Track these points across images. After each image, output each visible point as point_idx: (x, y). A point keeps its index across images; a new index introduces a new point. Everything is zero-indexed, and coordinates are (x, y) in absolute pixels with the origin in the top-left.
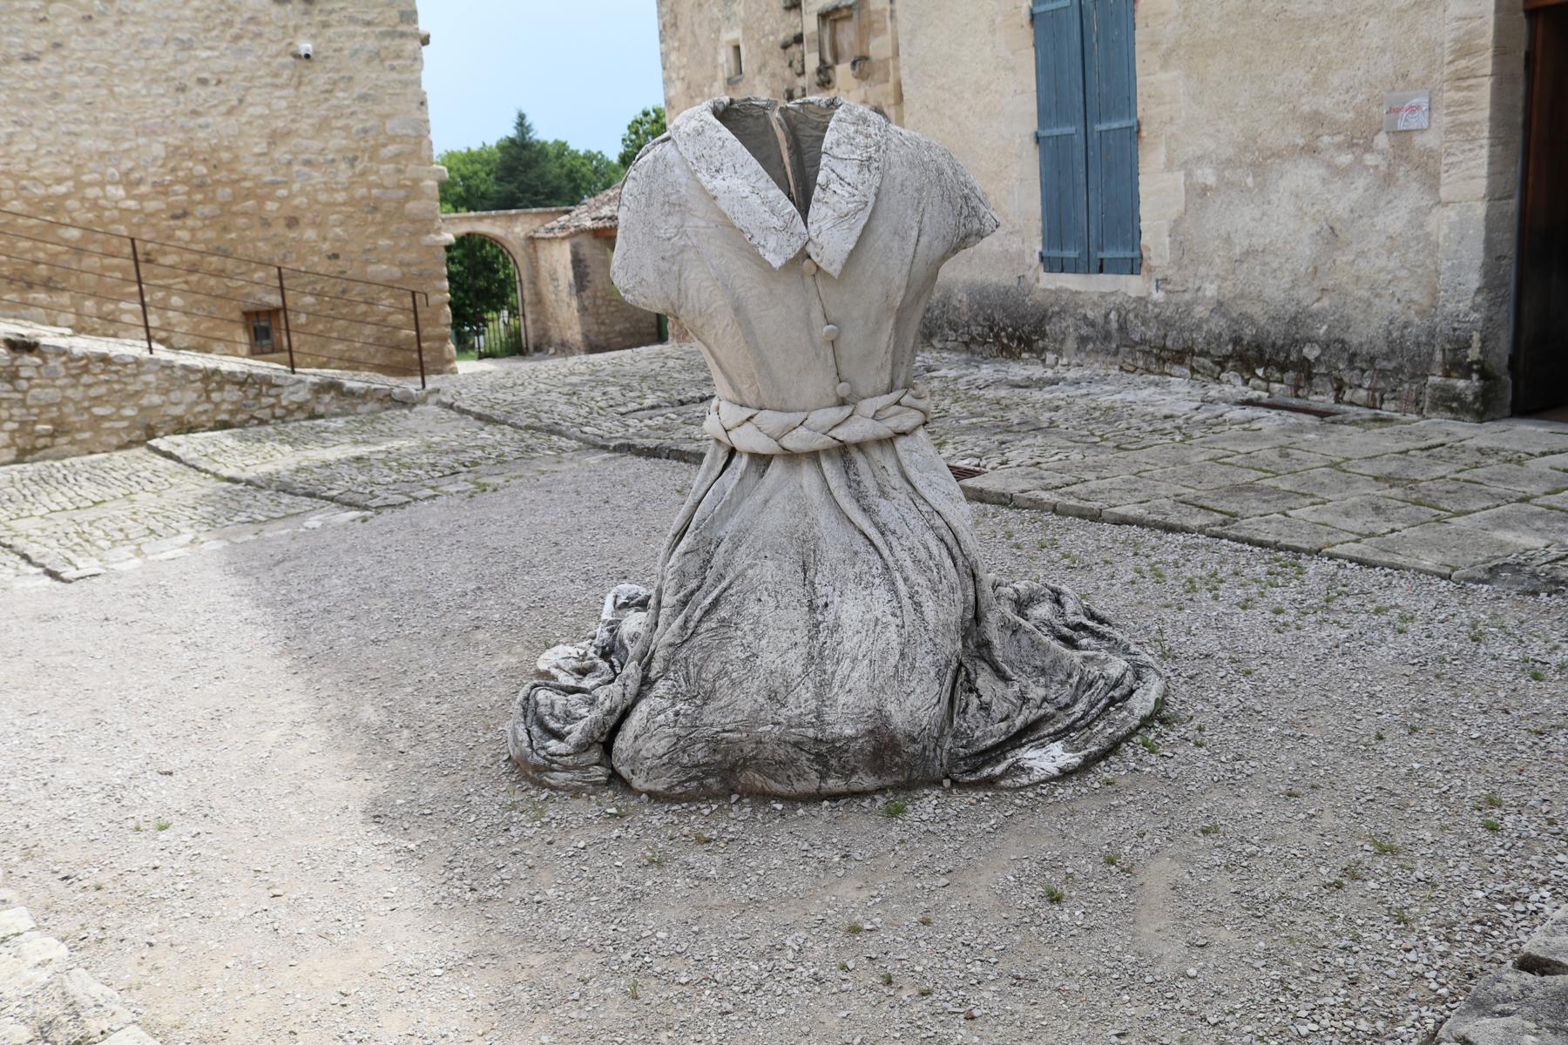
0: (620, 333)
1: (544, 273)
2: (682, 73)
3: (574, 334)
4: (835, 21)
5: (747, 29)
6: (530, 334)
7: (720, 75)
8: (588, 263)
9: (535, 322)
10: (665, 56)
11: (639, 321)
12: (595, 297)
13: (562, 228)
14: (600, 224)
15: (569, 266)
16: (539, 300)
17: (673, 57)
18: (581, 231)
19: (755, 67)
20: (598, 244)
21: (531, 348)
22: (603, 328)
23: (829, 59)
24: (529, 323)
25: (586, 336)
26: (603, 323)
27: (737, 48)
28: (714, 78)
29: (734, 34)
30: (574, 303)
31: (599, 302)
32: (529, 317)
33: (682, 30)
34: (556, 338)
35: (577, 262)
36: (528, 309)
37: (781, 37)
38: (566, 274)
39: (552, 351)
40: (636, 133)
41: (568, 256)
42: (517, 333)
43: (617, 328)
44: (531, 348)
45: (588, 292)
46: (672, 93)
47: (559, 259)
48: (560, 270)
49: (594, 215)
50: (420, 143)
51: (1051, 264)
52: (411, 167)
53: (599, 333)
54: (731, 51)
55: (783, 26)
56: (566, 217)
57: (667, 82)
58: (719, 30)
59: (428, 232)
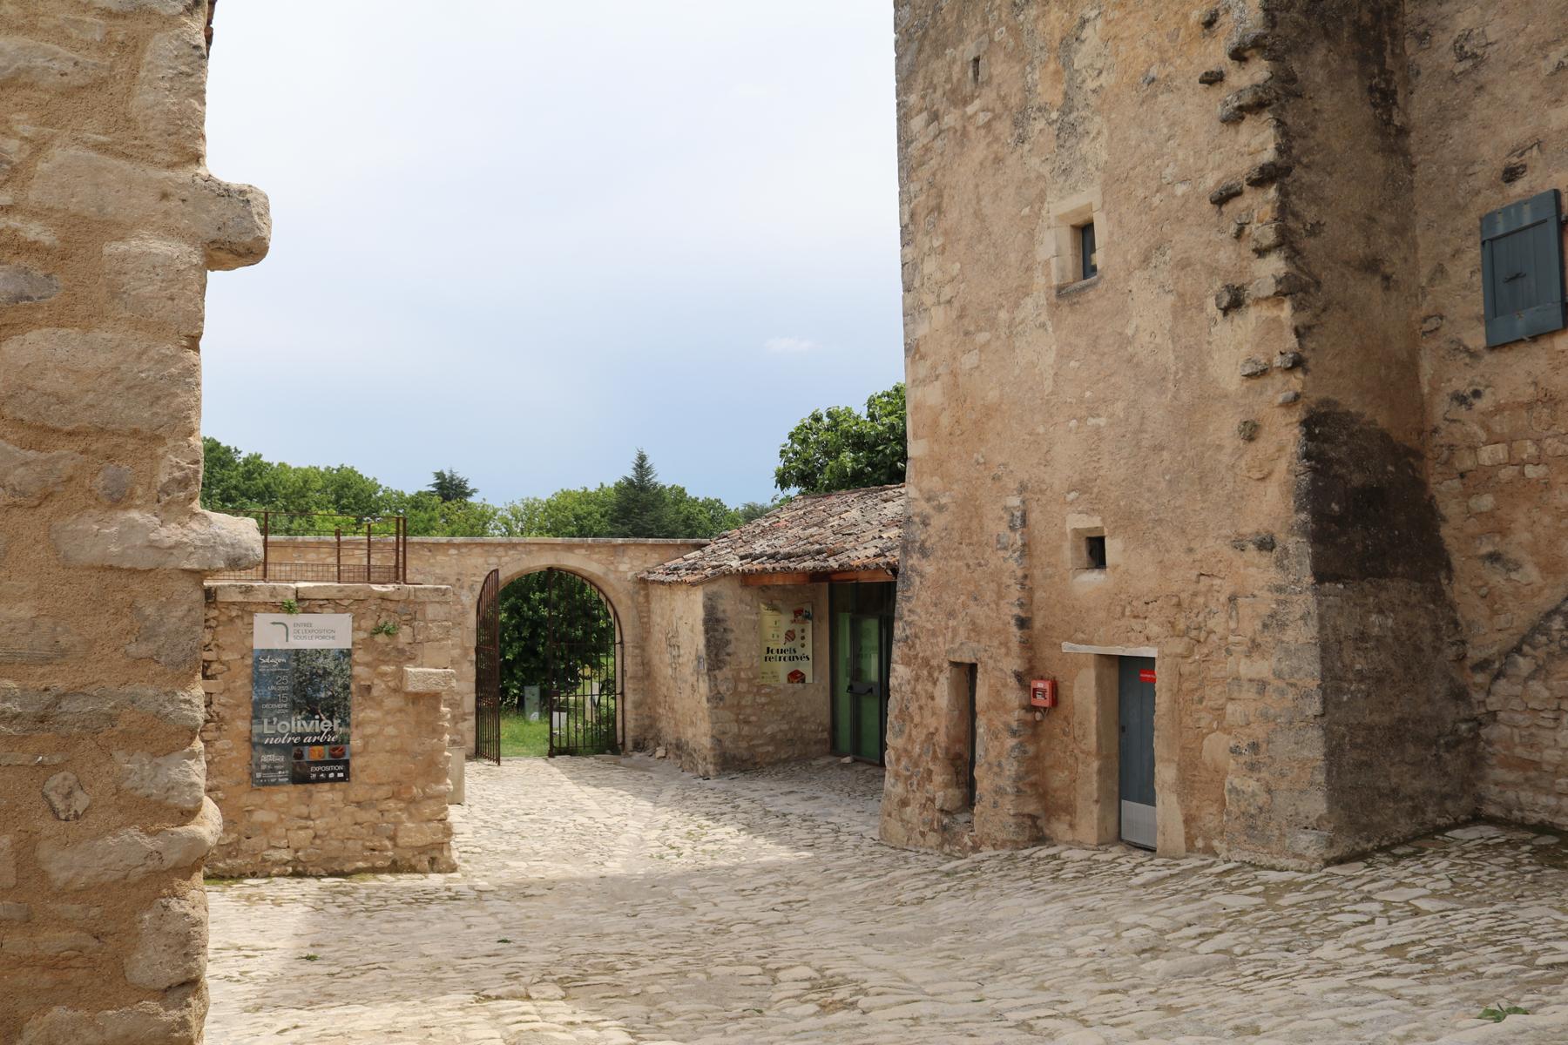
0: (773, 738)
1: (657, 635)
2: (947, 292)
3: (700, 734)
5: (1114, 181)
6: (630, 724)
7: (1040, 281)
8: (730, 624)
9: (638, 705)
10: (910, 268)
11: (802, 720)
12: (737, 680)
13: (692, 568)
14: (756, 566)
15: (700, 628)
16: (647, 673)
17: (930, 266)
18: (722, 574)
19: (1133, 256)
20: (746, 595)
21: (629, 745)
22: (746, 730)
24: (628, 706)
25: (717, 741)
26: (747, 722)
27: (1085, 231)
28: (1025, 291)
29: (1083, 198)
30: (704, 687)
31: (743, 687)
32: (630, 698)
33: (953, 215)
34: (669, 735)
35: (713, 621)
36: (629, 686)
37: (1211, 182)
38: (693, 640)
39: (660, 752)
40: (804, 441)
41: (699, 613)
42: (610, 719)
43: (768, 730)
44: (629, 745)
45: (727, 672)
46: (922, 330)
47: (683, 615)
48: (684, 631)
49: (742, 552)
50: (131, 47)
52: (60, 154)
53: (738, 737)
54: (1066, 239)
55: (1217, 157)
56: (698, 553)
57: (911, 314)
58: (1042, 197)
59: (119, 499)
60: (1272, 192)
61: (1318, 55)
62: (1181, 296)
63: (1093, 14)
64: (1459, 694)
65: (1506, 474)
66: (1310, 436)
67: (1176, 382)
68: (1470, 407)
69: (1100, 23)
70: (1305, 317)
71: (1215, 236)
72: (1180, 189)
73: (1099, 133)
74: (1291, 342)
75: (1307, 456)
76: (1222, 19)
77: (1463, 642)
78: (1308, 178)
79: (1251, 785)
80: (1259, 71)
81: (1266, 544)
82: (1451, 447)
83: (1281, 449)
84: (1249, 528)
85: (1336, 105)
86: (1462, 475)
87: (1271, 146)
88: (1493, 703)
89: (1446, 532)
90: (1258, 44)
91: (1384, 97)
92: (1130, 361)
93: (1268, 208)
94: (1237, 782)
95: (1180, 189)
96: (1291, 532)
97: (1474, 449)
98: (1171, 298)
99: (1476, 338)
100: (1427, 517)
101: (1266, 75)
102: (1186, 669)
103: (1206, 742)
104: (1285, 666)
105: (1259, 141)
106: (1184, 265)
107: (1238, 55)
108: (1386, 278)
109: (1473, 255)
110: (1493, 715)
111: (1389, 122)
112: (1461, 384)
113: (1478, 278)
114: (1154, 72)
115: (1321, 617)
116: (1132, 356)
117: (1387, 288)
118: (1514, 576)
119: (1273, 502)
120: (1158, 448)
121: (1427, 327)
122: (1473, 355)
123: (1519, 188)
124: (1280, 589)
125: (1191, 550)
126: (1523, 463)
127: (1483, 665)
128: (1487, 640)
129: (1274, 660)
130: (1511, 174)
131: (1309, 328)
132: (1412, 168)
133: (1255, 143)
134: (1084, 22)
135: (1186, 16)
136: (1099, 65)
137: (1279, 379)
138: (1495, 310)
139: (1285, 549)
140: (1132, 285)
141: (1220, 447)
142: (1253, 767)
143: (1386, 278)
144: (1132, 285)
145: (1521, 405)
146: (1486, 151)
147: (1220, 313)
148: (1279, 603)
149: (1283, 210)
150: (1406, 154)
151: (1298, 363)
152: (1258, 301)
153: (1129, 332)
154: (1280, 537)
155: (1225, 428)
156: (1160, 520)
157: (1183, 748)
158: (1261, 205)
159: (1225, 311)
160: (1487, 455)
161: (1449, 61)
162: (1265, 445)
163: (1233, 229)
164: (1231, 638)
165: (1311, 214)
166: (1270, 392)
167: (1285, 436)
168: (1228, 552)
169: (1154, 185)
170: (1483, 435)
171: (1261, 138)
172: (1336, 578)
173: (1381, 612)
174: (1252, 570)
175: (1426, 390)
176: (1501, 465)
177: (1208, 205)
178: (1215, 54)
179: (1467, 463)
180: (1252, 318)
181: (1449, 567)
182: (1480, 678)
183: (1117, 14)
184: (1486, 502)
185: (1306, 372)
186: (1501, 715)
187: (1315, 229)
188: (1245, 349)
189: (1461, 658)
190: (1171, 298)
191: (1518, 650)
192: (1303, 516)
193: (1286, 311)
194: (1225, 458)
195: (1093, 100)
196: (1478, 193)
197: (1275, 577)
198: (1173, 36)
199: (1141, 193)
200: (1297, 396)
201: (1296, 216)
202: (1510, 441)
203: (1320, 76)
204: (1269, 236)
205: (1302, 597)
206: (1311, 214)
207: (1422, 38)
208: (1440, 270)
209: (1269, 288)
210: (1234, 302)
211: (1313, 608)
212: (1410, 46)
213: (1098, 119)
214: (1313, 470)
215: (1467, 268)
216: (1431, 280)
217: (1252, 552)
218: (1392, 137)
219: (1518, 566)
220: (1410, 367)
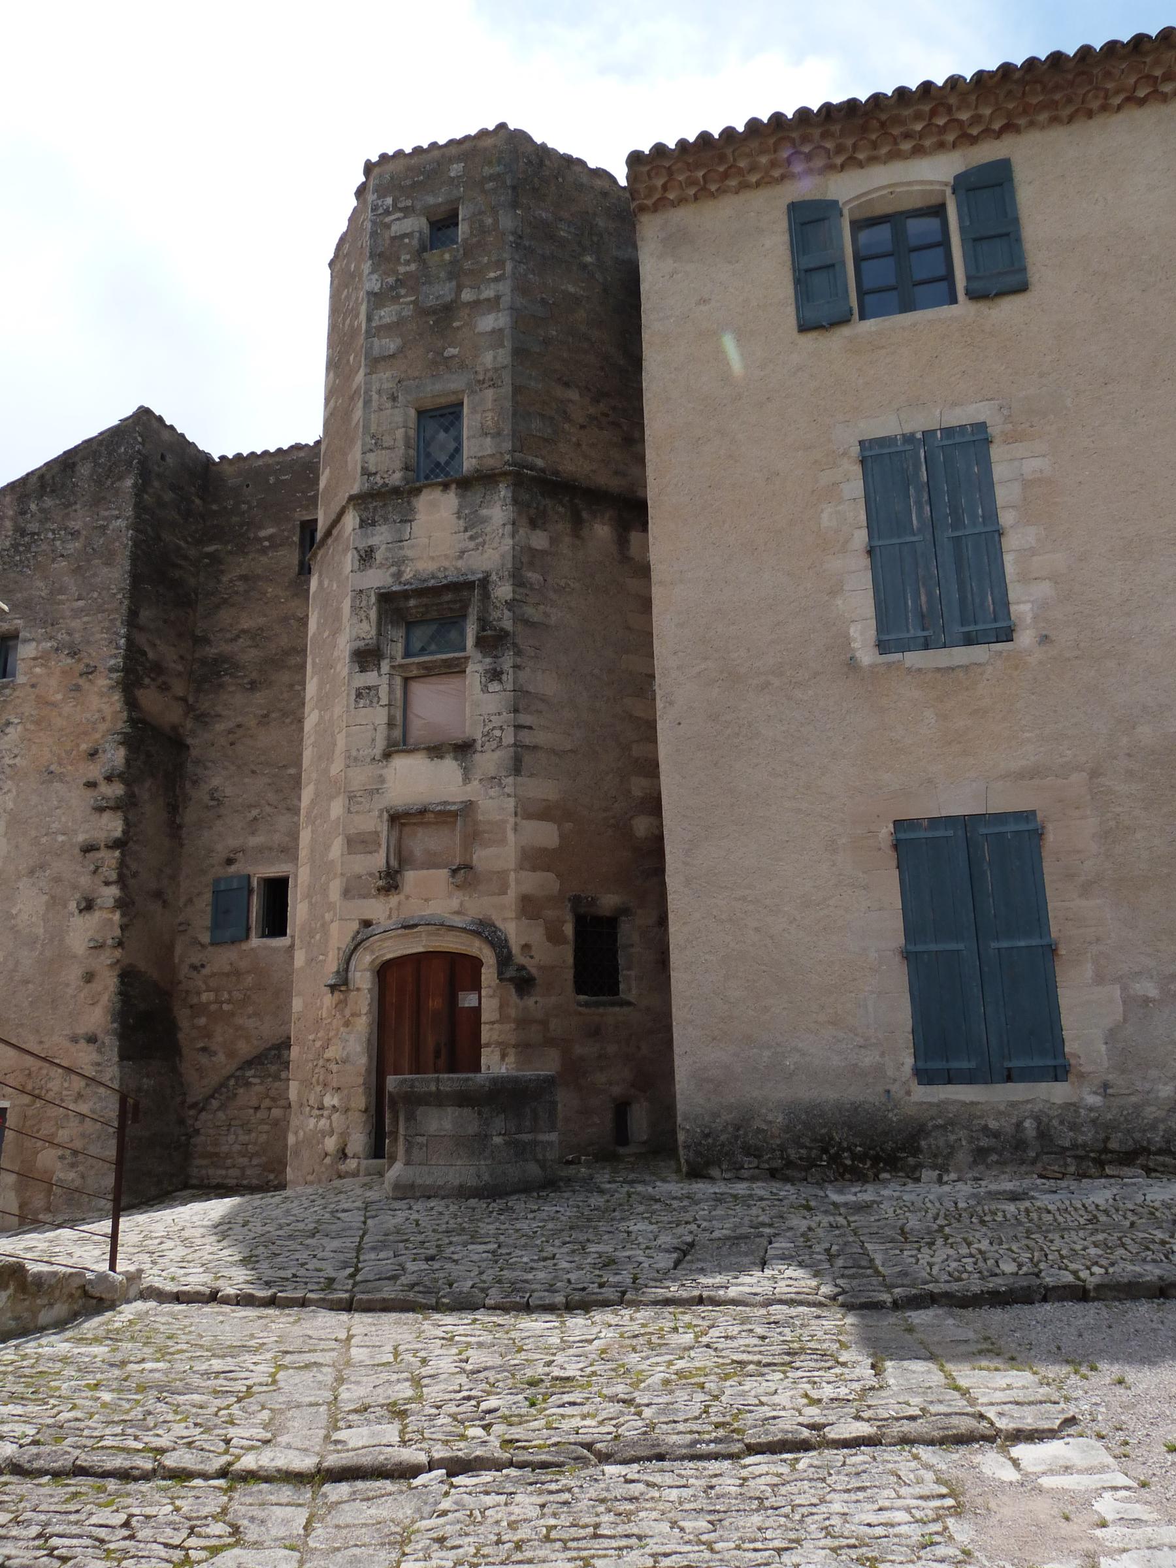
4: (403, 824)
23: (394, 863)
37: (81, 838)
51: (924, 1076)
60: (117, 853)
61: (147, 785)
62: (53, 897)
63: (16, 721)
64: (181, 1122)
65: (213, 1007)
66: (122, 983)
67: (43, 945)
68: (199, 972)
69: (20, 728)
70: (125, 920)
71: (79, 868)
72: (61, 838)
73: (9, 791)
74: (118, 932)
75: (120, 993)
76: (100, 754)
77: (185, 1094)
78: (136, 847)
79: (72, 1175)
80: (117, 790)
81: (92, 1039)
82: (187, 992)
83: (106, 988)
84: (81, 1030)
85: (152, 811)
86: (191, 1007)
87: (120, 829)
88: (198, 1125)
89: (181, 1036)
90: (121, 776)
91: (173, 808)
92: (12, 928)
93: (114, 861)
94: (61, 1175)
95: (61, 838)
96: (107, 1033)
97: (199, 994)
98: (46, 897)
99: (205, 938)
100: (172, 1027)
101: (122, 792)
102: (30, 1112)
103: (39, 1155)
104: (98, 1106)
105: (113, 825)
106: (57, 880)
107: (109, 779)
108: (164, 902)
109: (208, 896)
110: (197, 1132)
111: (174, 822)
112: (195, 960)
113: (209, 908)
114: (52, 768)
115: (121, 1079)
116: (15, 926)
117: (164, 907)
118: (213, 1059)
119: (97, 1016)
120: (27, 982)
121: (181, 928)
122: (203, 946)
123: (233, 869)
124: (98, 1064)
125: (41, 1042)
126: (222, 1003)
127: (194, 1106)
128: (197, 1092)
129: (91, 1103)
130: (230, 862)
131: (127, 926)
132: (182, 845)
133: (111, 825)
134: (8, 724)
135: (78, 745)
136: (16, 752)
137: (108, 952)
138: (216, 926)
139: (103, 1043)
140: (20, 885)
141: (67, 985)
142: (73, 1165)
143: (164, 902)
144: (20, 885)
145: (223, 974)
146: (219, 847)
147: (77, 911)
148: (97, 1072)
149: (122, 864)
150: (180, 838)
151: (120, 944)
152: (101, 908)
153: (14, 912)
154: (101, 1036)
155: (74, 974)
156: (22, 1025)
157: (22, 1162)
158: (111, 858)
159: (81, 911)
160: (205, 997)
161: (206, 798)
162: (97, 986)
163: (92, 867)
164: (65, 1093)
165: (134, 866)
166: (102, 958)
167: (108, 983)
168: (67, 1044)
169: (44, 831)
170: (204, 987)
171: (114, 824)
172: (129, 1059)
173: (148, 1076)
174: (81, 1054)
175: (177, 961)
176: (209, 1003)
177: (77, 851)
178: (95, 771)
179: (195, 1001)
180: (96, 917)
181: (181, 1055)
182: (192, 1112)
183: (32, 727)
184: (202, 1021)
185: (123, 949)
186: (202, 1131)
187: (135, 875)
188: (89, 933)
189: (183, 1102)
190: (46, 897)
191: (212, 1096)
192: (115, 1025)
193: (117, 917)
194: (70, 991)
195: (8, 770)
196: (213, 866)
197: (95, 1057)
198: (69, 753)
199: (33, 833)
200: (118, 961)
201: (128, 867)
202: (217, 991)
203: (146, 796)
204: (114, 876)
205: (110, 1069)
206: (134, 866)
207: (195, 783)
208: (190, 901)
209: (110, 903)
210: (88, 906)
211: (117, 1074)
212: (188, 785)
213: (9, 782)
214: (122, 1001)
215: (204, 902)
216: (185, 905)
217: (83, 1044)
218: (175, 830)
219: (215, 1053)
220: (170, 948)
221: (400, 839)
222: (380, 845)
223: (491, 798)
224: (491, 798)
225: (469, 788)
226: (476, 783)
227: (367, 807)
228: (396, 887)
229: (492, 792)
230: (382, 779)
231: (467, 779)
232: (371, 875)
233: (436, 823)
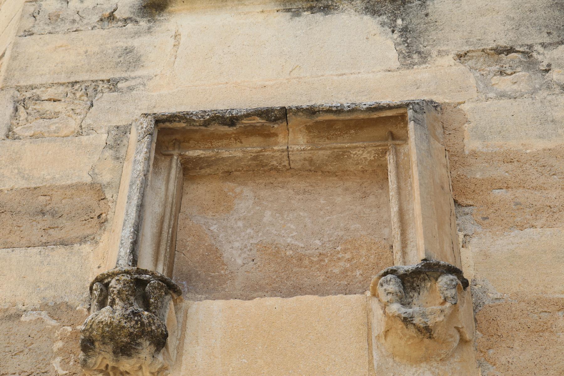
4: (189, 170)
221: (176, 208)
222: (102, 221)
223: (502, 95)
224: (502, 95)
225: (422, 73)
226: (449, 60)
227: (73, 124)
228: (160, 342)
229: (504, 84)
230: (131, 58)
231: (412, 48)
232: (56, 310)
233: (313, 170)
